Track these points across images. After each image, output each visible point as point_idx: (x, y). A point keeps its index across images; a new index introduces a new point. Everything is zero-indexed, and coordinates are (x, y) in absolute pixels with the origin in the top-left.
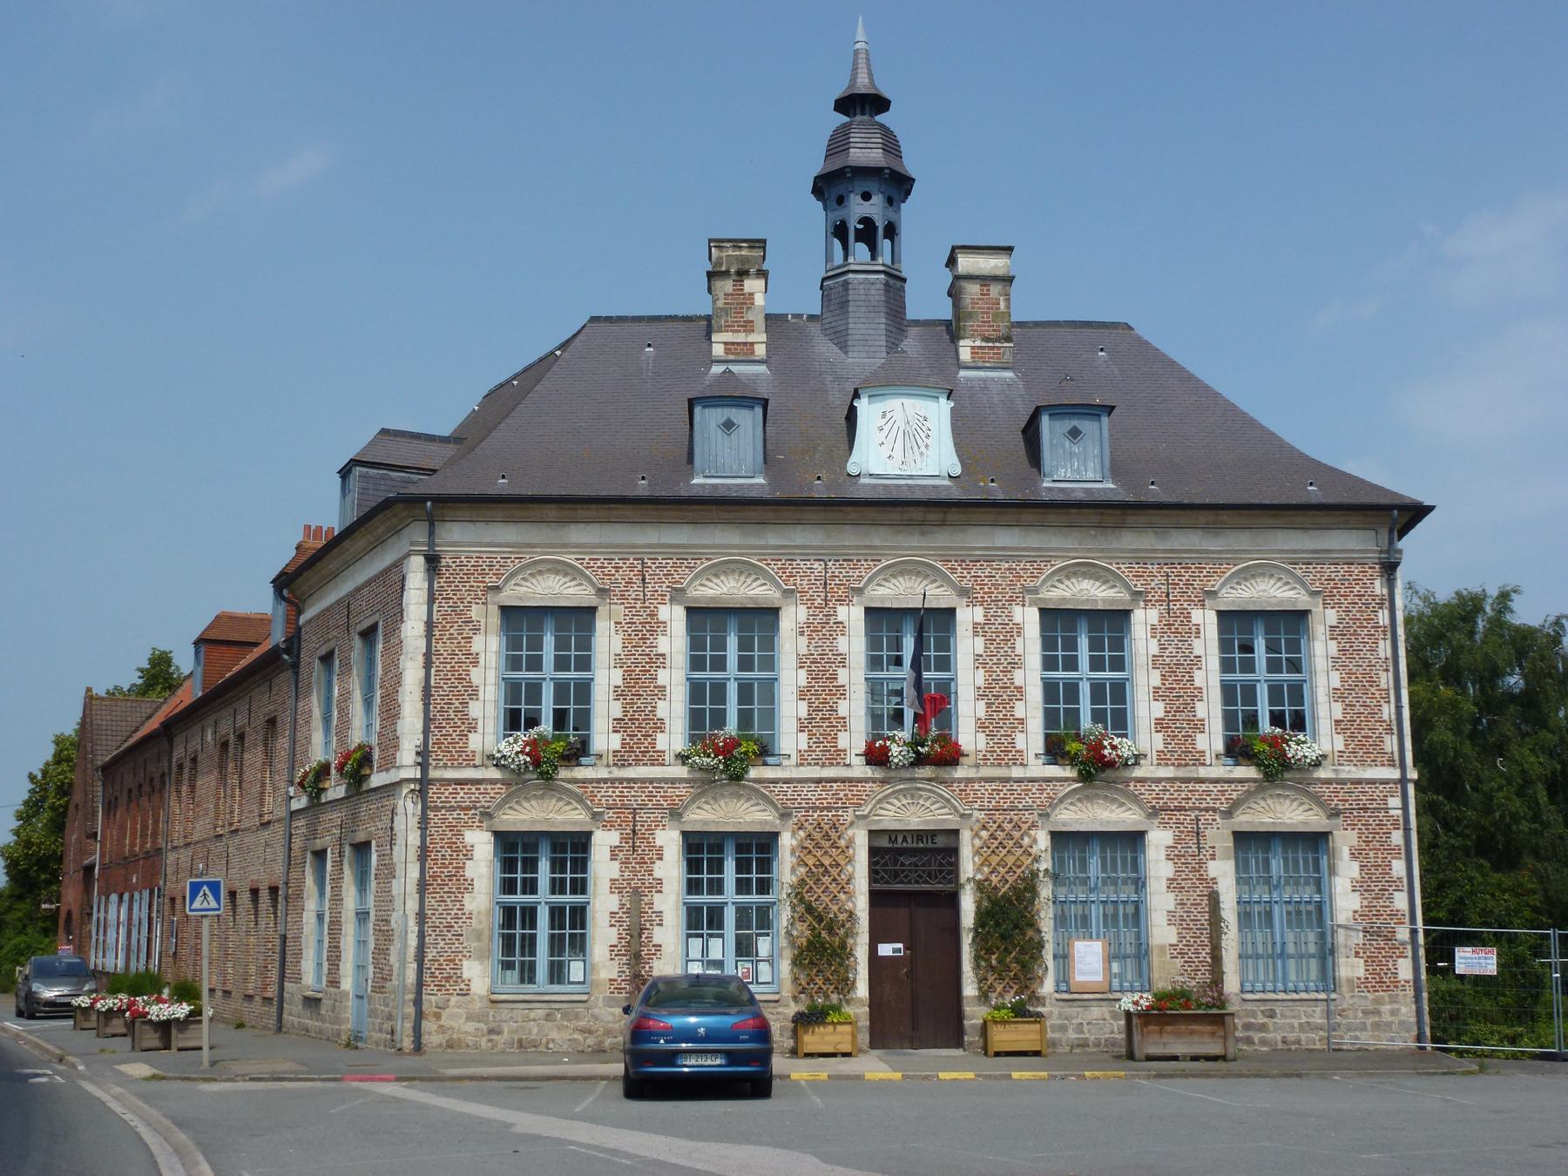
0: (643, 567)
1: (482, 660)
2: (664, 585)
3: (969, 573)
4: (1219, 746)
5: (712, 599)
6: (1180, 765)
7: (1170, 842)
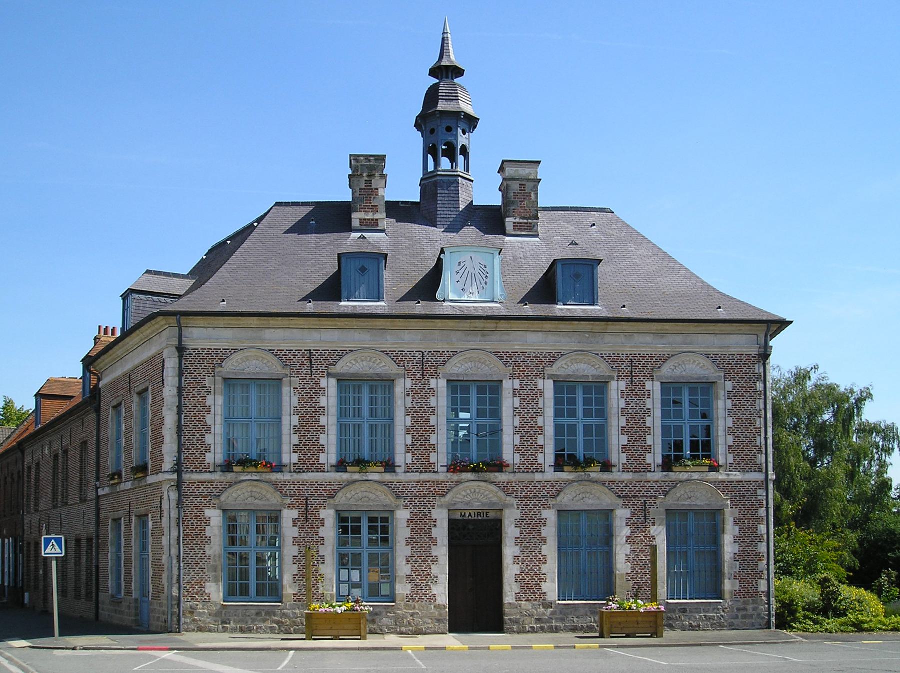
0: (311, 355)
1: (213, 410)
2: (324, 366)
3: (511, 359)
4: (659, 460)
7: (629, 516)
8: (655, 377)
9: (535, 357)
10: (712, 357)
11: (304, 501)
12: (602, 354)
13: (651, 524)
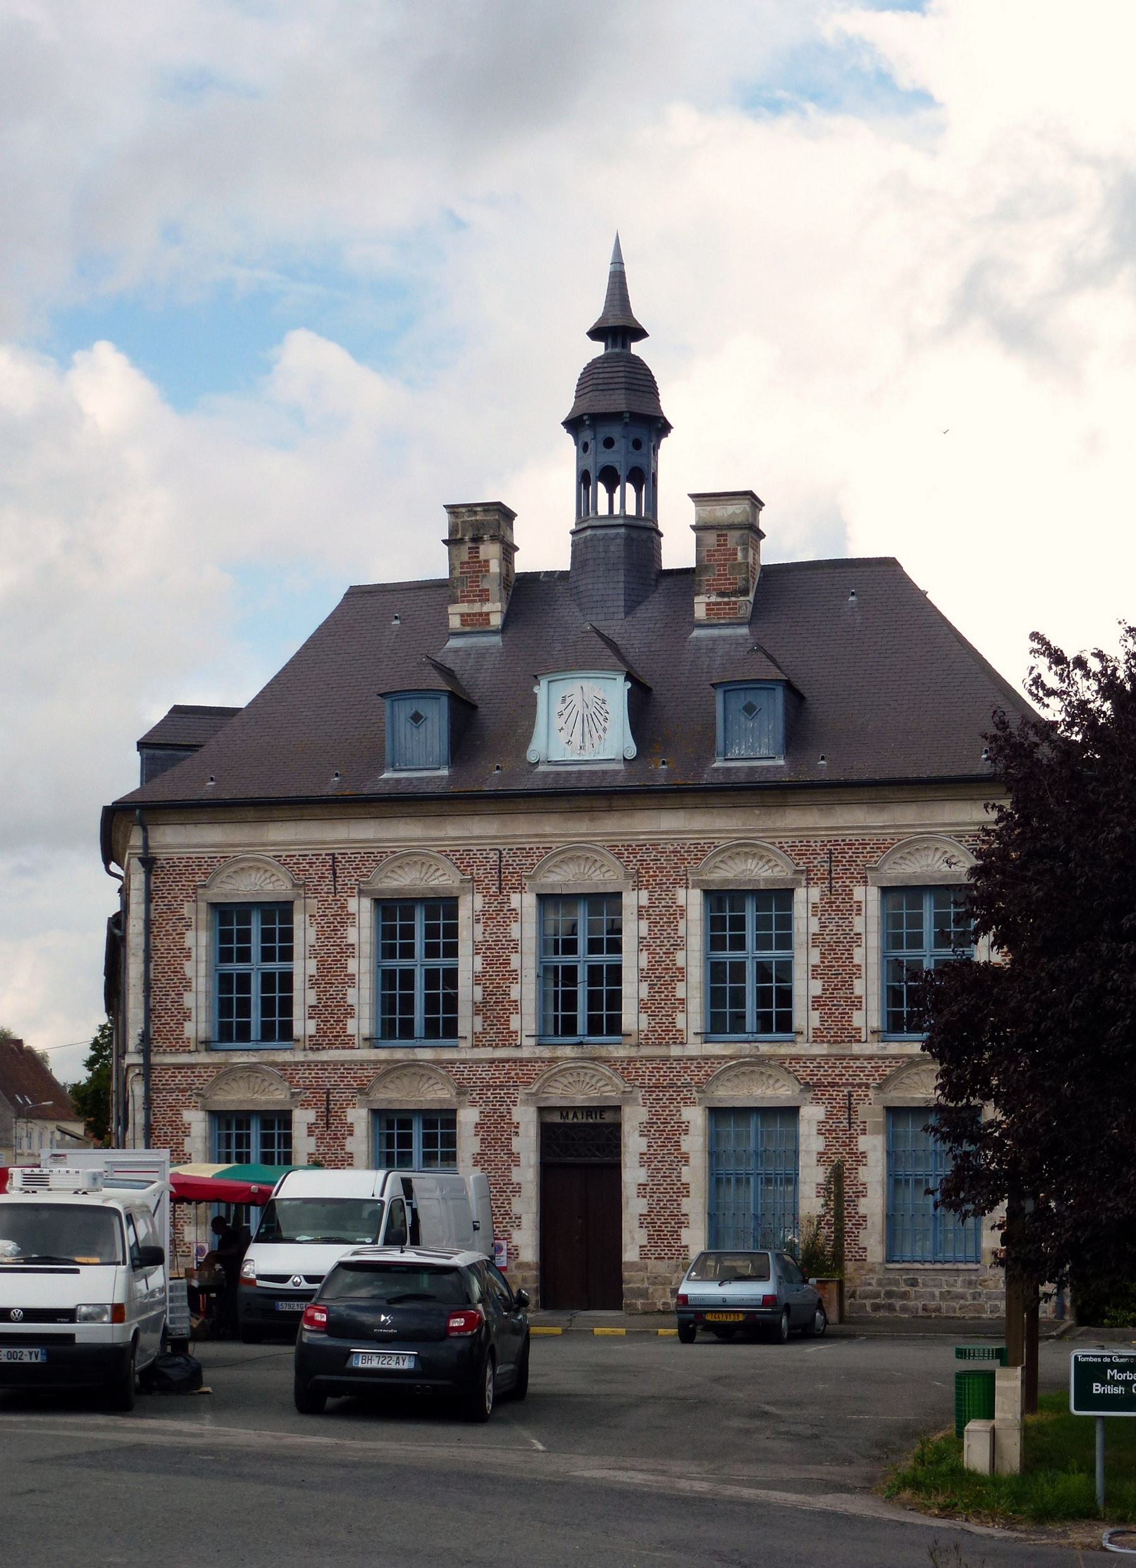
0: (334, 862)
1: (193, 954)
2: (353, 878)
3: (635, 857)
5: (396, 890)
6: (835, 1042)
7: (822, 1117)
8: (869, 880)
9: (673, 852)
10: (967, 841)
11: (325, 1095)
12: (781, 843)
13: (859, 1132)
